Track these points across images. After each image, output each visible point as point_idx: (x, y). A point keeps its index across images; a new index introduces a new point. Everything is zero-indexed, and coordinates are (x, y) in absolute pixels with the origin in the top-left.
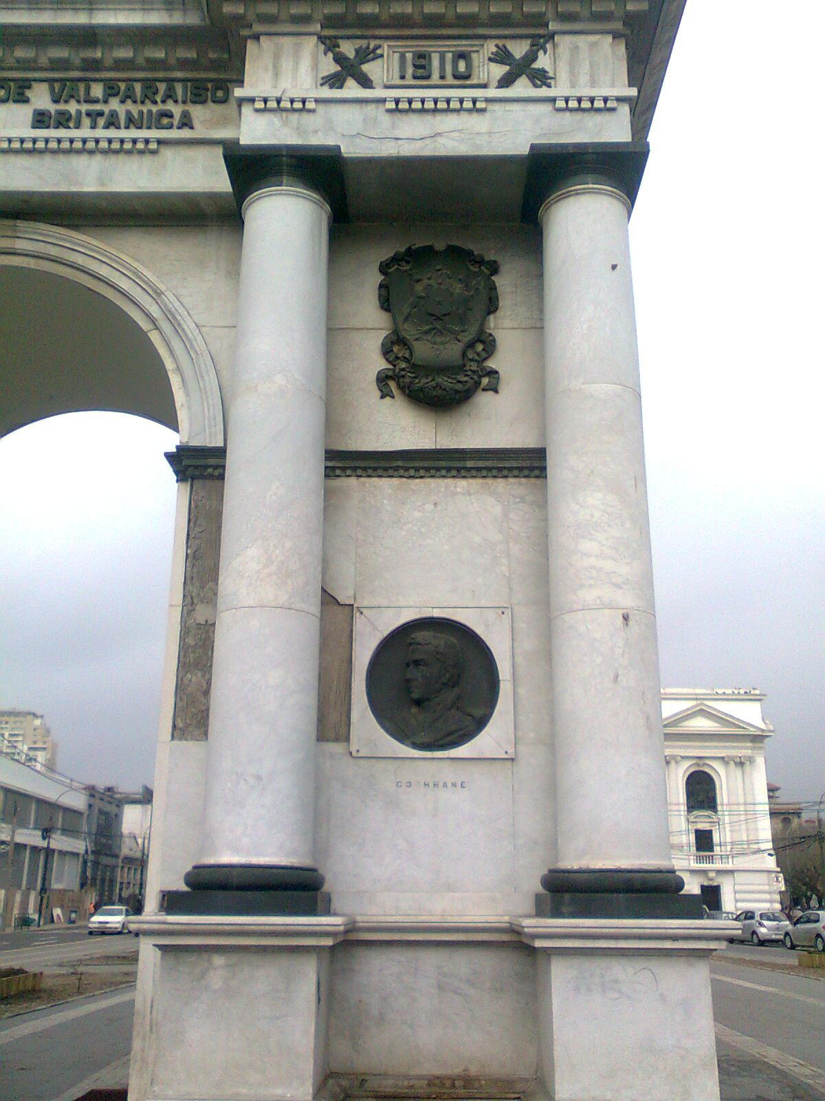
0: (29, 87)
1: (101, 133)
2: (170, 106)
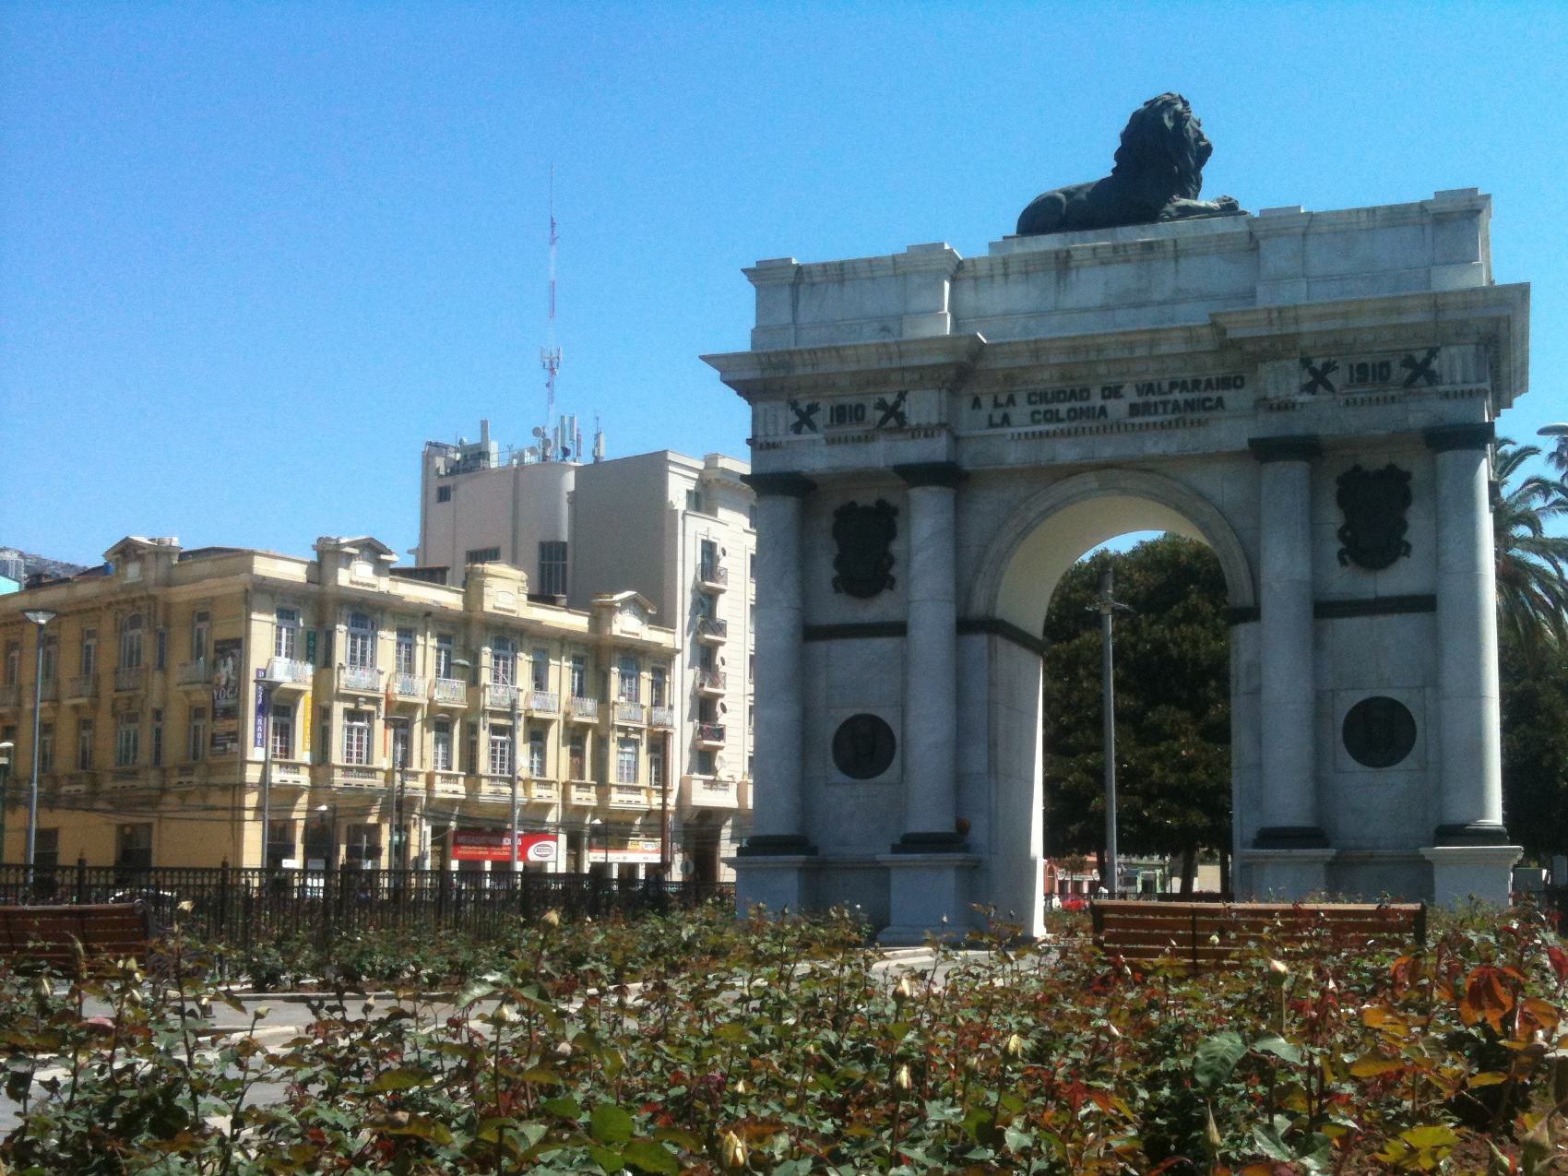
0: (1121, 387)
1: (1169, 417)
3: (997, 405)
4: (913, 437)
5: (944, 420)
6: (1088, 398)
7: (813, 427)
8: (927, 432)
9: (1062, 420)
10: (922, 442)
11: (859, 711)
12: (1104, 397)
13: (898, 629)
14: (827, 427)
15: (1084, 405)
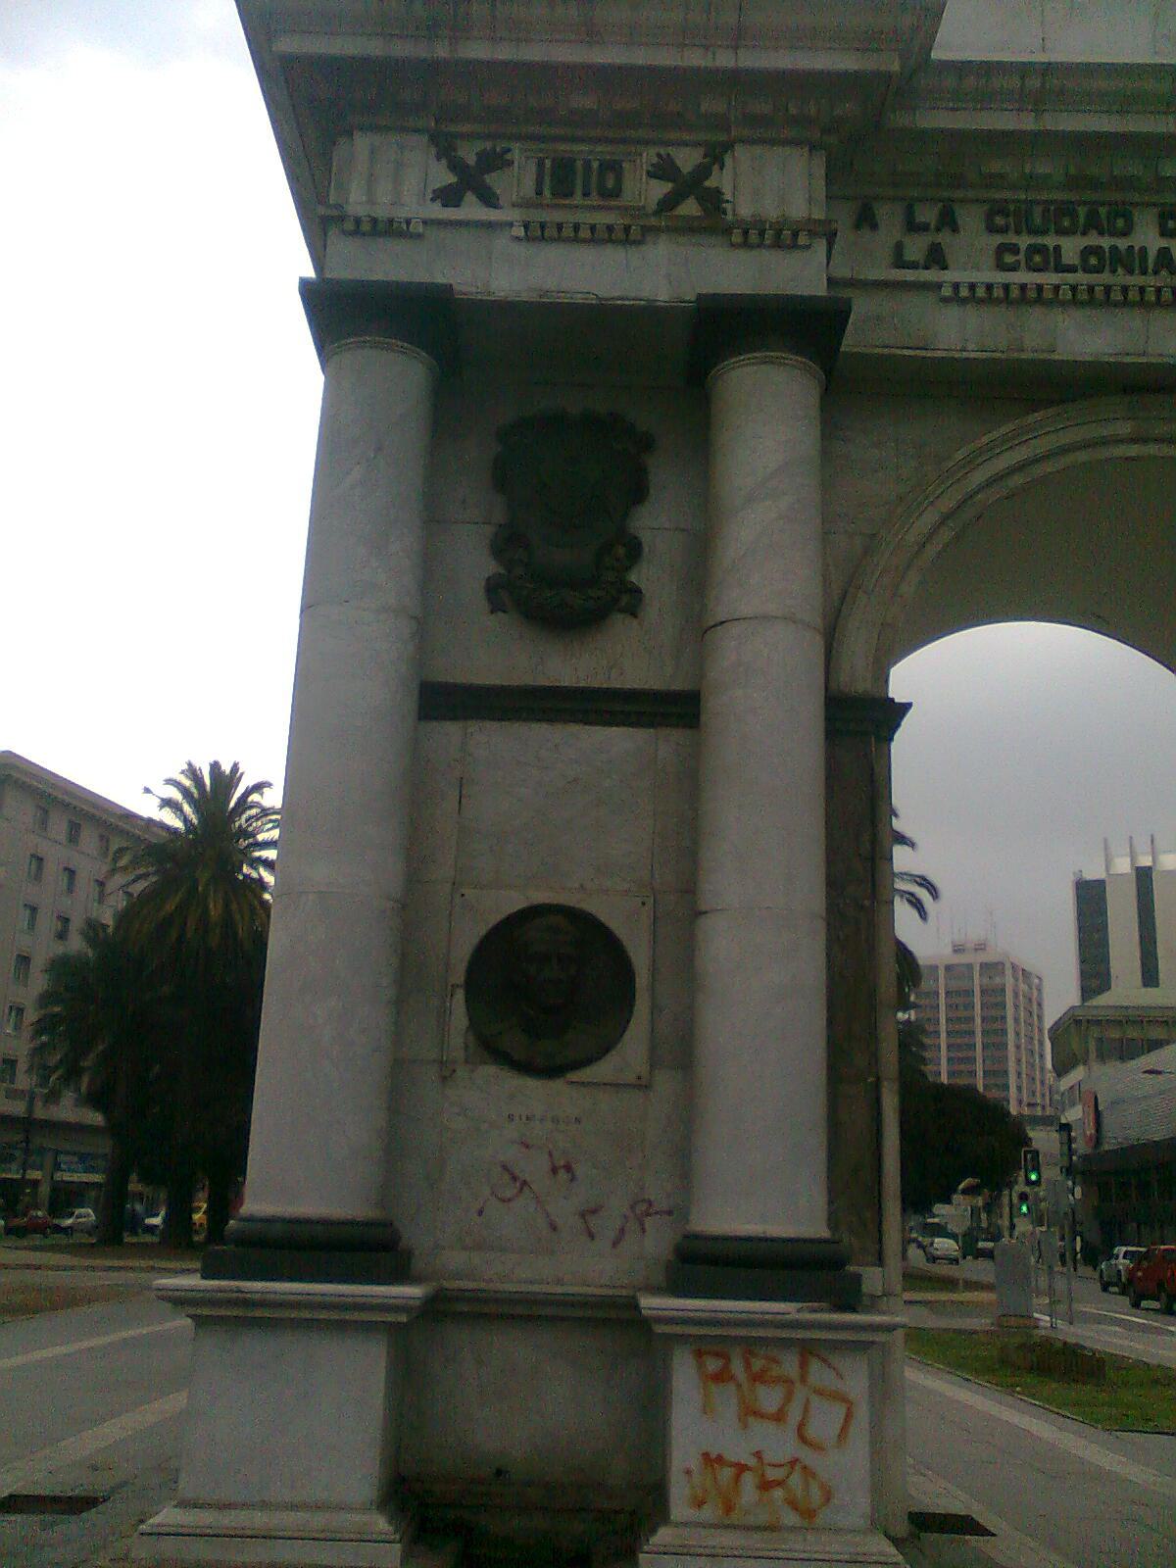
3: (913, 227)
4: (746, 245)
5: (819, 214)
7: (489, 199)
8: (782, 236)
9: (1071, 269)
10: (769, 257)
11: (540, 897)
14: (524, 204)
15: (1122, 244)
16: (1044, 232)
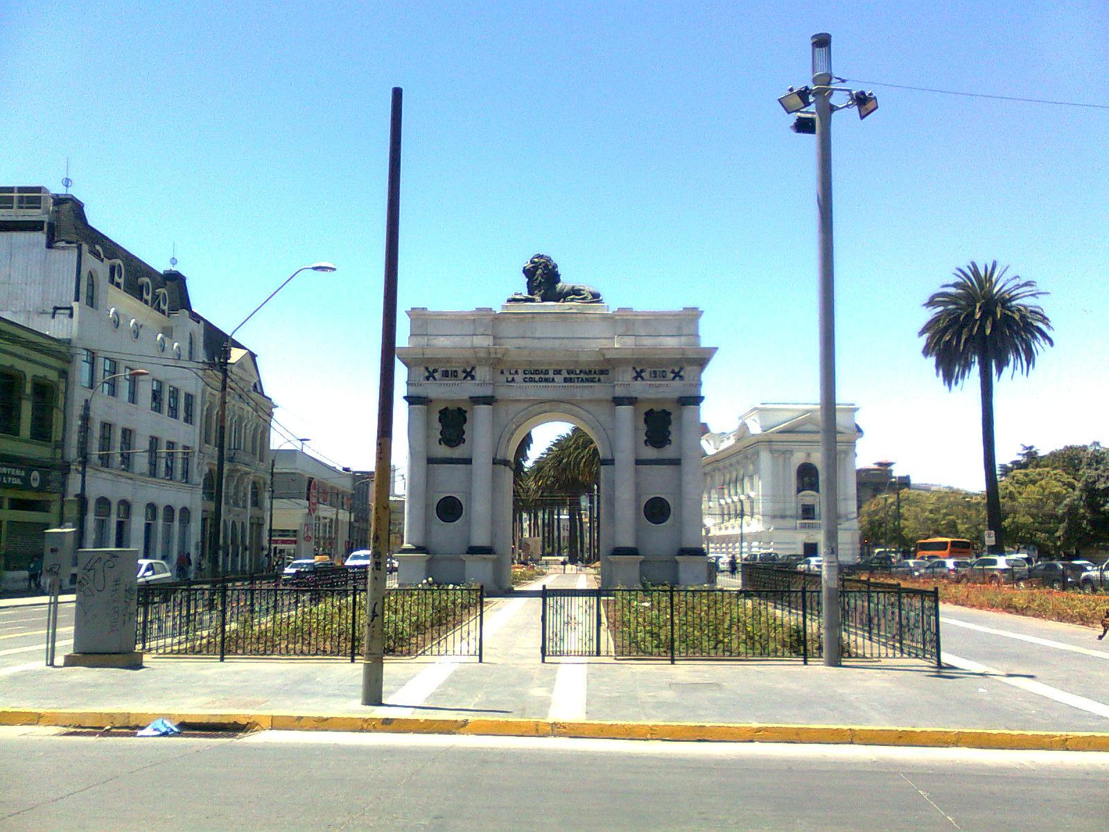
2: (595, 376)
6: (548, 374)
8: (484, 384)
9: (536, 382)
12: (554, 374)
13: (468, 461)
15: (547, 376)
16: (533, 374)
